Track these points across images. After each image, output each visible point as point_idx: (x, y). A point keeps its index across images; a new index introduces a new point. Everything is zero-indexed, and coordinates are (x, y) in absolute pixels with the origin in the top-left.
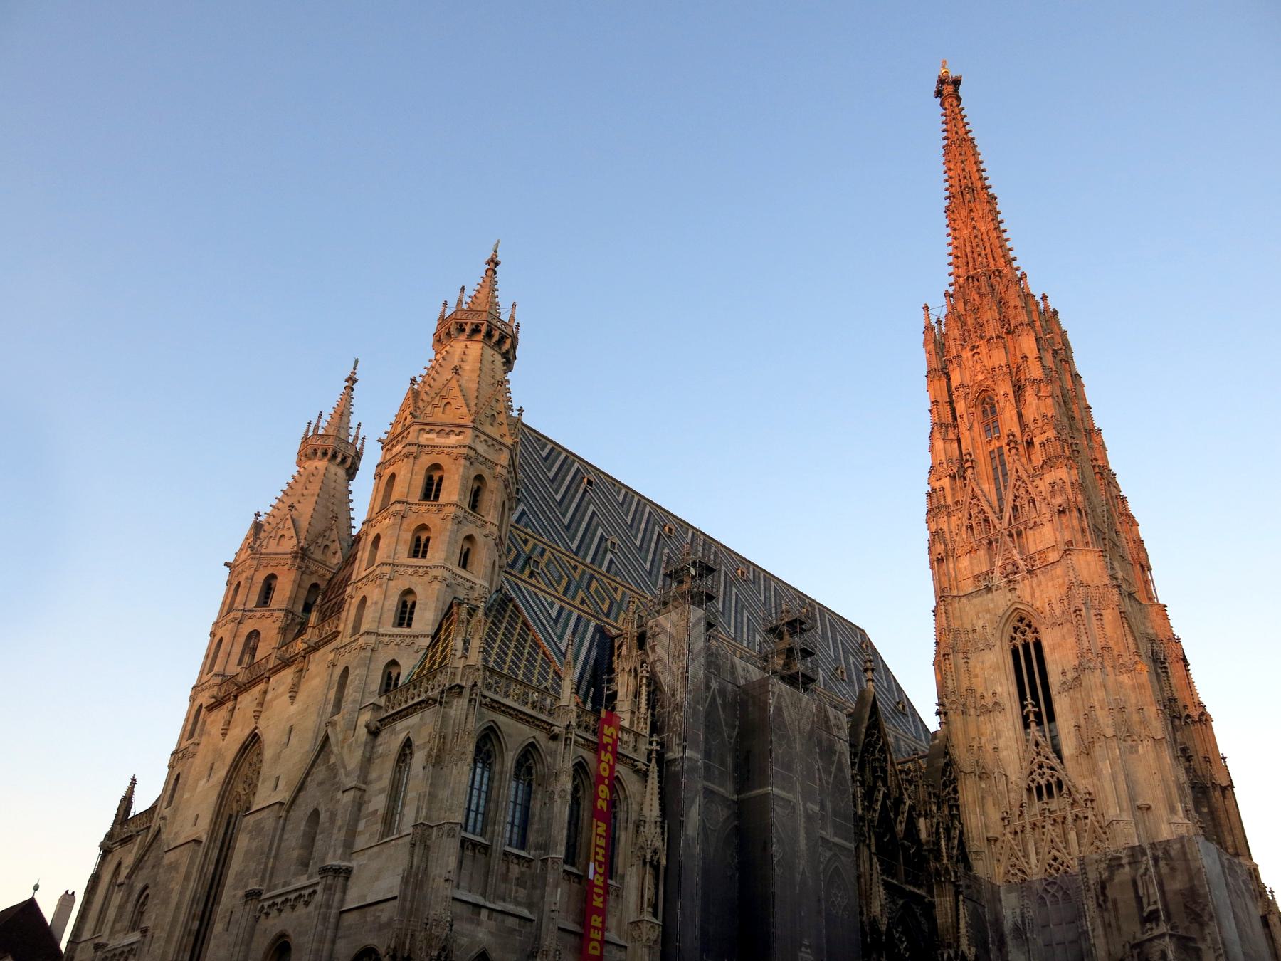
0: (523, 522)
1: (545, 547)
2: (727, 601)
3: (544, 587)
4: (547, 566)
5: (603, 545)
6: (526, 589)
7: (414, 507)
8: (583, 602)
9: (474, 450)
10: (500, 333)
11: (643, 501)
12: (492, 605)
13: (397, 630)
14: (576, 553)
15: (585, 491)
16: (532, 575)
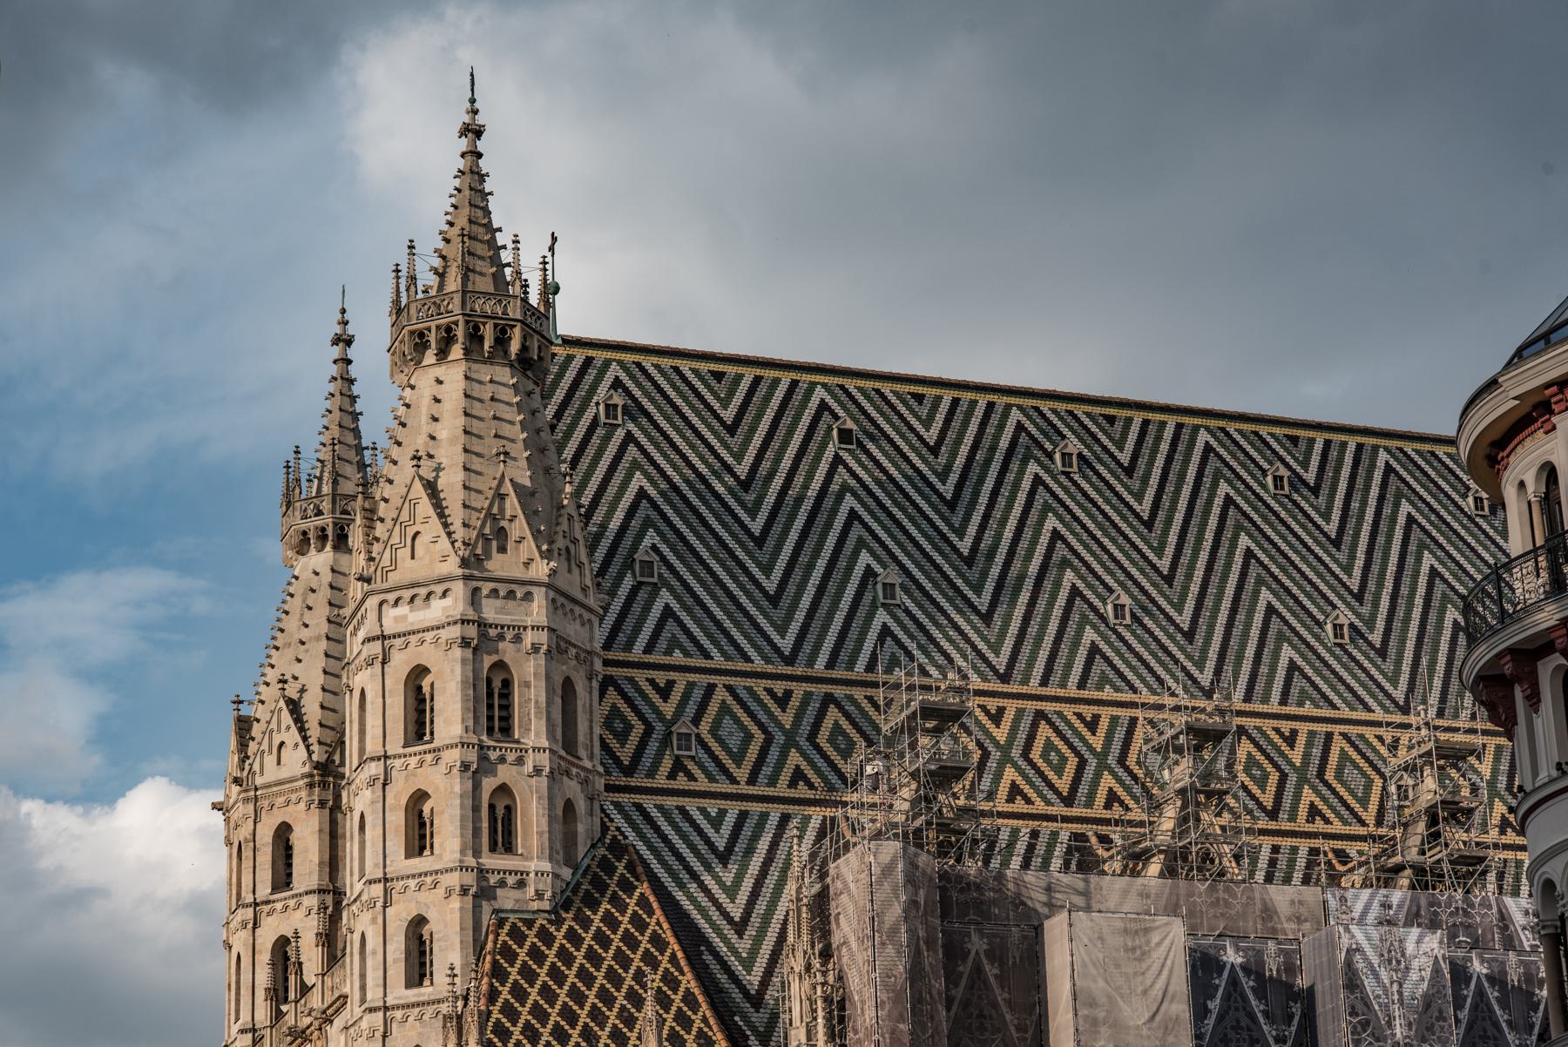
0: (662, 644)
1: (713, 679)
2: (1212, 590)
3: (703, 784)
4: (713, 732)
5: (867, 598)
6: (660, 808)
7: (398, 763)
8: (798, 776)
9: (474, 622)
10: (496, 326)
11: (1001, 401)
12: (578, 884)
13: (413, 995)
14: (790, 660)
15: (837, 460)
16: (678, 767)
